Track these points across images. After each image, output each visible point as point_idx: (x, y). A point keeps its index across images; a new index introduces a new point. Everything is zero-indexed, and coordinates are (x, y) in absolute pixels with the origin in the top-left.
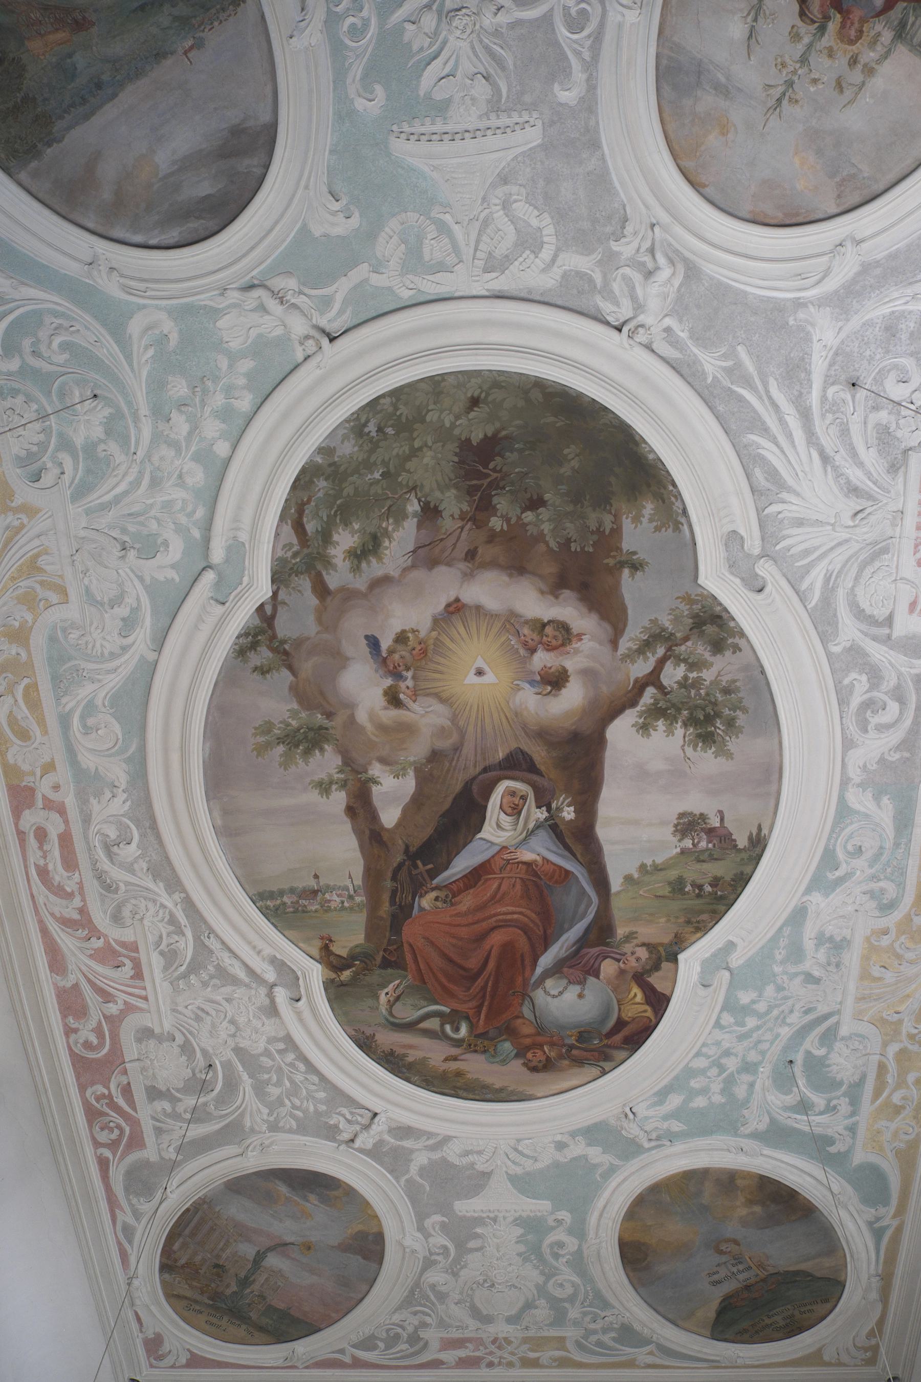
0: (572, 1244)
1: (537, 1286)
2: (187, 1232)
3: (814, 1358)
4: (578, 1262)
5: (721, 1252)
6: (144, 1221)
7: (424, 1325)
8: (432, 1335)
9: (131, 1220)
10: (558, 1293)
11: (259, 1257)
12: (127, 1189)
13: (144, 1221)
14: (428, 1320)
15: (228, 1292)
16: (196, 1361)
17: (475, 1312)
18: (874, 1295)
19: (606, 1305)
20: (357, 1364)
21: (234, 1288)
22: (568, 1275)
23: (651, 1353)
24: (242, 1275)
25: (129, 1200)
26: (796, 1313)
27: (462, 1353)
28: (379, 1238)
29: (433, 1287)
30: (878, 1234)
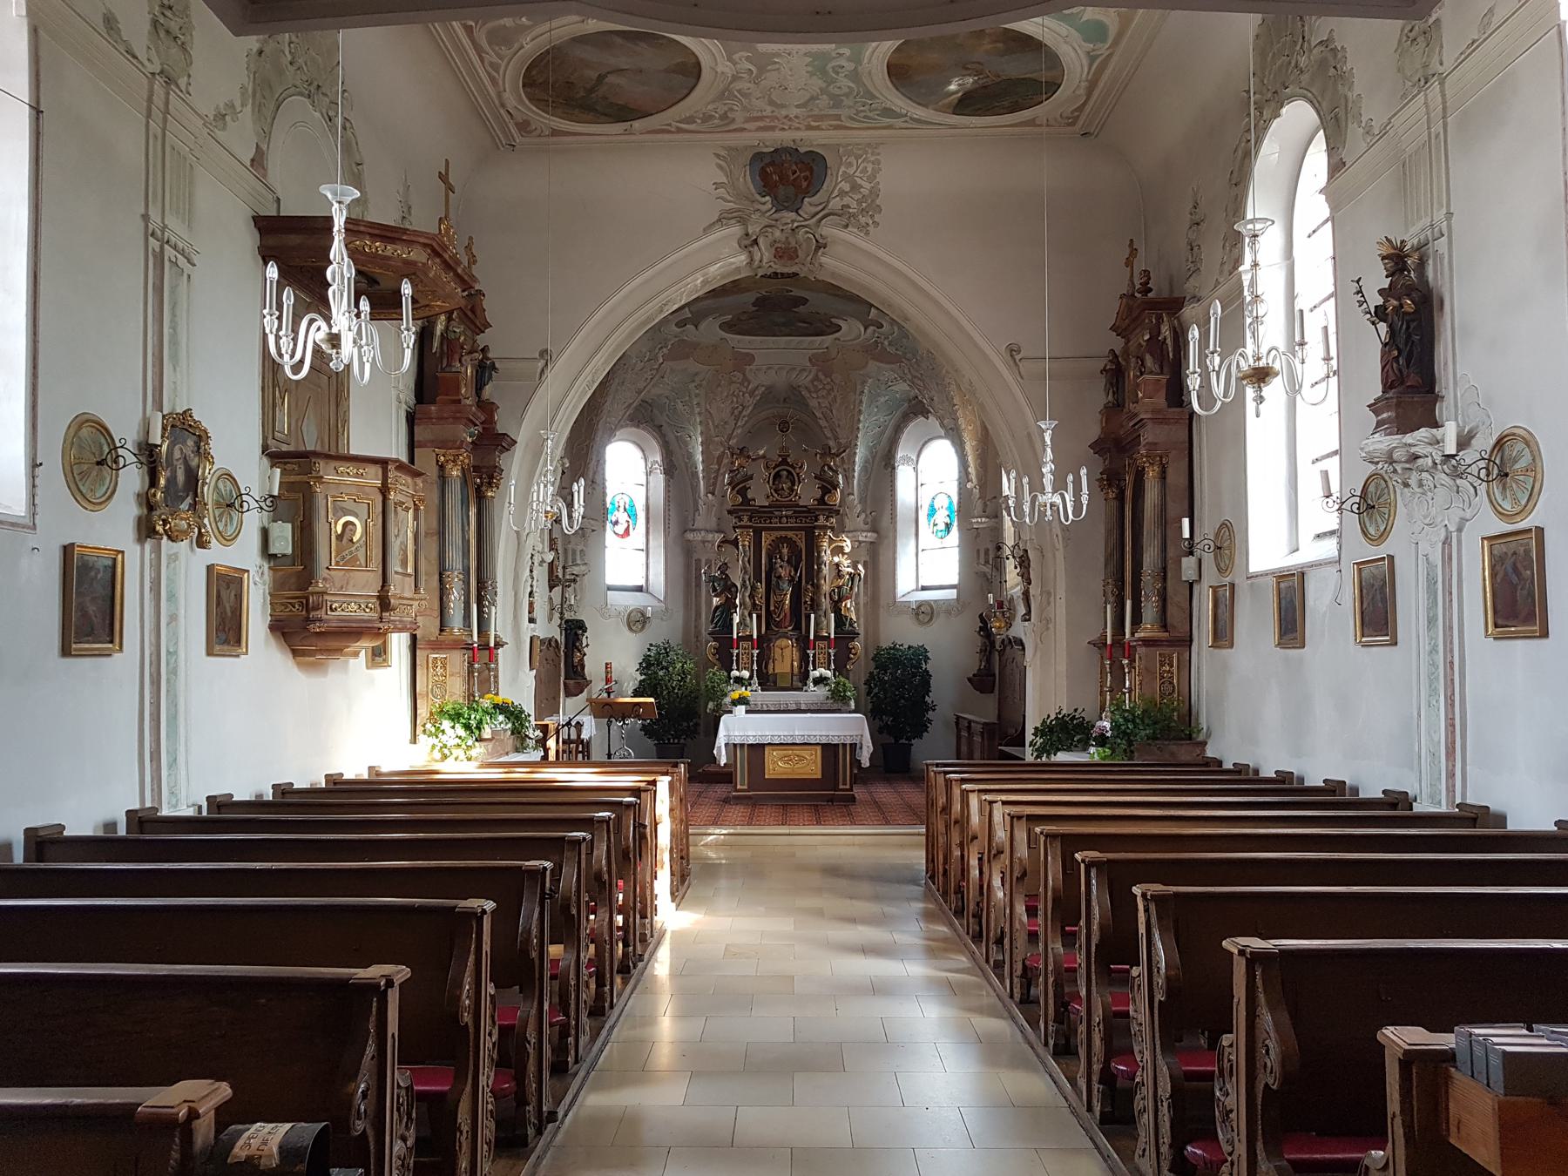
0: (850, 66)
1: (821, 89)
2: (542, 64)
3: (1031, 123)
4: (855, 76)
5: (967, 69)
6: (506, 61)
7: (731, 109)
8: (739, 116)
9: (495, 59)
10: (837, 91)
11: (601, 78)
12: (490, 44)
13: (506, 61)
14: (735, 108)
15: (578, 96)
16: (555, 133)
17: (771, 103)
18: (1082, 91)
19: (873, 97)
20: (679, 130)
21: (582, 93)
22: (845, 83)
23: (906, 121)
24: (588, 86)
25: (494, 51)
26: (1020, 100)
27: (761, 124)
28: (698, 65)
29: (739, 91)
30: (1092, 59)
